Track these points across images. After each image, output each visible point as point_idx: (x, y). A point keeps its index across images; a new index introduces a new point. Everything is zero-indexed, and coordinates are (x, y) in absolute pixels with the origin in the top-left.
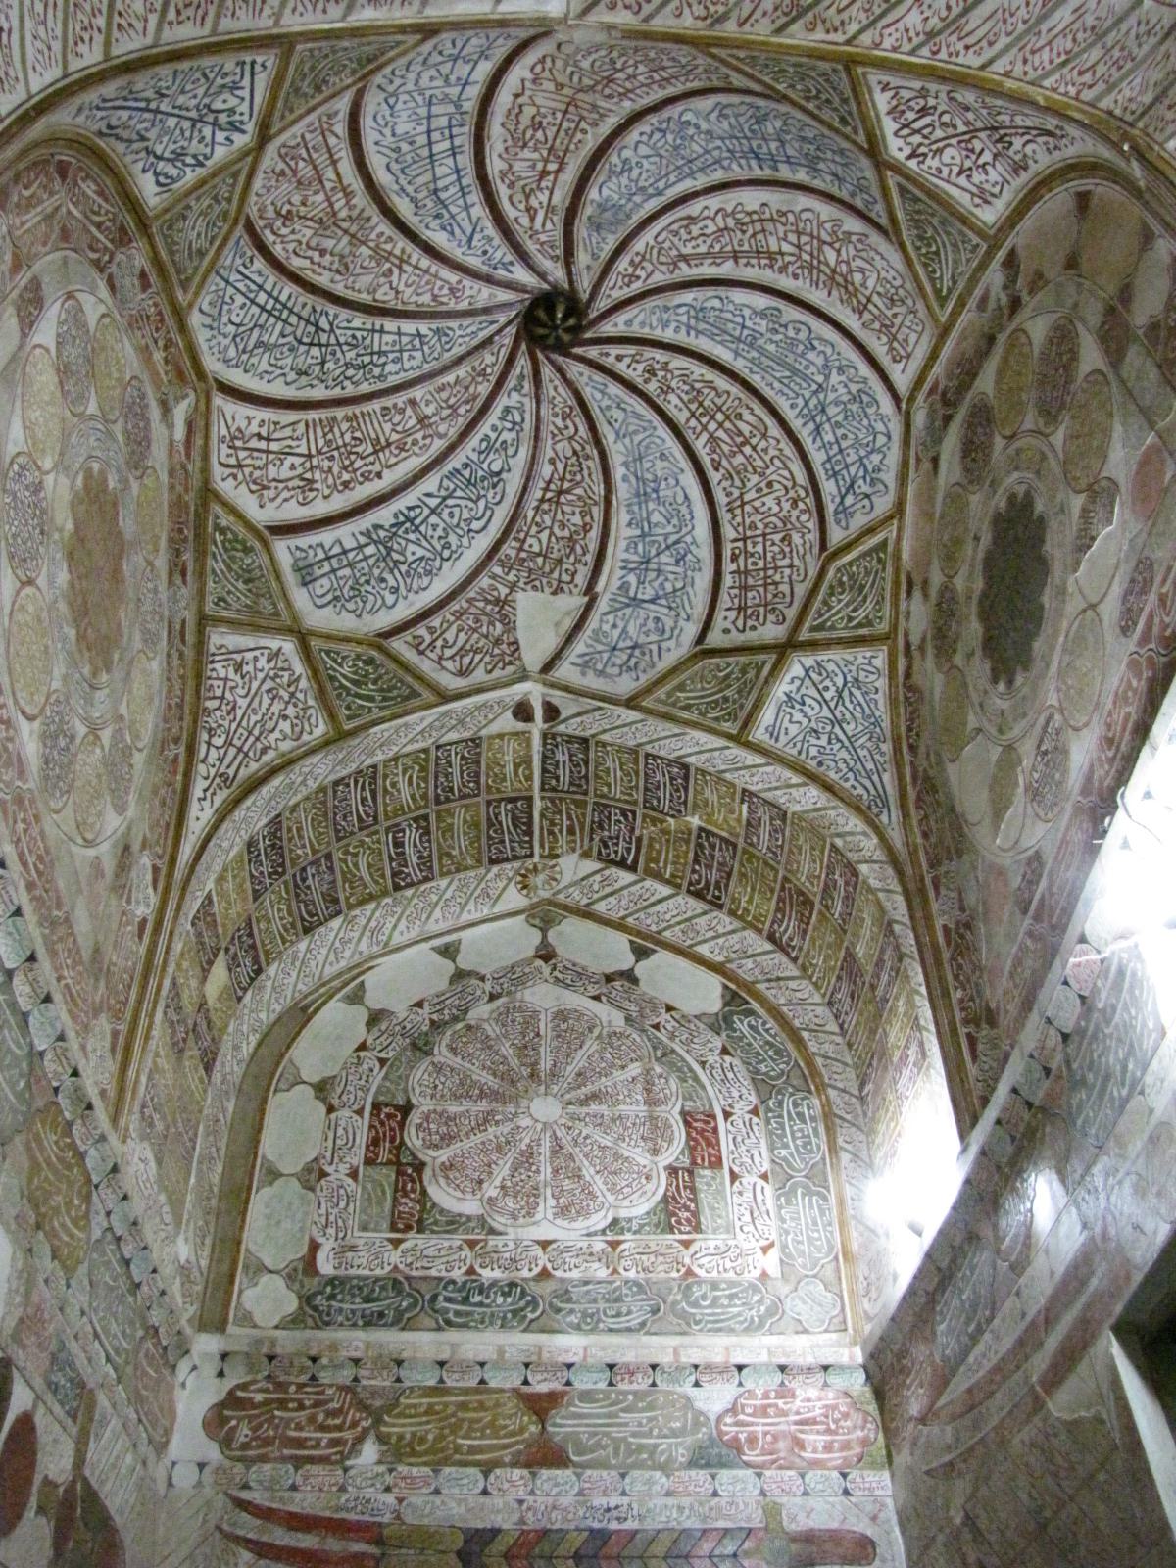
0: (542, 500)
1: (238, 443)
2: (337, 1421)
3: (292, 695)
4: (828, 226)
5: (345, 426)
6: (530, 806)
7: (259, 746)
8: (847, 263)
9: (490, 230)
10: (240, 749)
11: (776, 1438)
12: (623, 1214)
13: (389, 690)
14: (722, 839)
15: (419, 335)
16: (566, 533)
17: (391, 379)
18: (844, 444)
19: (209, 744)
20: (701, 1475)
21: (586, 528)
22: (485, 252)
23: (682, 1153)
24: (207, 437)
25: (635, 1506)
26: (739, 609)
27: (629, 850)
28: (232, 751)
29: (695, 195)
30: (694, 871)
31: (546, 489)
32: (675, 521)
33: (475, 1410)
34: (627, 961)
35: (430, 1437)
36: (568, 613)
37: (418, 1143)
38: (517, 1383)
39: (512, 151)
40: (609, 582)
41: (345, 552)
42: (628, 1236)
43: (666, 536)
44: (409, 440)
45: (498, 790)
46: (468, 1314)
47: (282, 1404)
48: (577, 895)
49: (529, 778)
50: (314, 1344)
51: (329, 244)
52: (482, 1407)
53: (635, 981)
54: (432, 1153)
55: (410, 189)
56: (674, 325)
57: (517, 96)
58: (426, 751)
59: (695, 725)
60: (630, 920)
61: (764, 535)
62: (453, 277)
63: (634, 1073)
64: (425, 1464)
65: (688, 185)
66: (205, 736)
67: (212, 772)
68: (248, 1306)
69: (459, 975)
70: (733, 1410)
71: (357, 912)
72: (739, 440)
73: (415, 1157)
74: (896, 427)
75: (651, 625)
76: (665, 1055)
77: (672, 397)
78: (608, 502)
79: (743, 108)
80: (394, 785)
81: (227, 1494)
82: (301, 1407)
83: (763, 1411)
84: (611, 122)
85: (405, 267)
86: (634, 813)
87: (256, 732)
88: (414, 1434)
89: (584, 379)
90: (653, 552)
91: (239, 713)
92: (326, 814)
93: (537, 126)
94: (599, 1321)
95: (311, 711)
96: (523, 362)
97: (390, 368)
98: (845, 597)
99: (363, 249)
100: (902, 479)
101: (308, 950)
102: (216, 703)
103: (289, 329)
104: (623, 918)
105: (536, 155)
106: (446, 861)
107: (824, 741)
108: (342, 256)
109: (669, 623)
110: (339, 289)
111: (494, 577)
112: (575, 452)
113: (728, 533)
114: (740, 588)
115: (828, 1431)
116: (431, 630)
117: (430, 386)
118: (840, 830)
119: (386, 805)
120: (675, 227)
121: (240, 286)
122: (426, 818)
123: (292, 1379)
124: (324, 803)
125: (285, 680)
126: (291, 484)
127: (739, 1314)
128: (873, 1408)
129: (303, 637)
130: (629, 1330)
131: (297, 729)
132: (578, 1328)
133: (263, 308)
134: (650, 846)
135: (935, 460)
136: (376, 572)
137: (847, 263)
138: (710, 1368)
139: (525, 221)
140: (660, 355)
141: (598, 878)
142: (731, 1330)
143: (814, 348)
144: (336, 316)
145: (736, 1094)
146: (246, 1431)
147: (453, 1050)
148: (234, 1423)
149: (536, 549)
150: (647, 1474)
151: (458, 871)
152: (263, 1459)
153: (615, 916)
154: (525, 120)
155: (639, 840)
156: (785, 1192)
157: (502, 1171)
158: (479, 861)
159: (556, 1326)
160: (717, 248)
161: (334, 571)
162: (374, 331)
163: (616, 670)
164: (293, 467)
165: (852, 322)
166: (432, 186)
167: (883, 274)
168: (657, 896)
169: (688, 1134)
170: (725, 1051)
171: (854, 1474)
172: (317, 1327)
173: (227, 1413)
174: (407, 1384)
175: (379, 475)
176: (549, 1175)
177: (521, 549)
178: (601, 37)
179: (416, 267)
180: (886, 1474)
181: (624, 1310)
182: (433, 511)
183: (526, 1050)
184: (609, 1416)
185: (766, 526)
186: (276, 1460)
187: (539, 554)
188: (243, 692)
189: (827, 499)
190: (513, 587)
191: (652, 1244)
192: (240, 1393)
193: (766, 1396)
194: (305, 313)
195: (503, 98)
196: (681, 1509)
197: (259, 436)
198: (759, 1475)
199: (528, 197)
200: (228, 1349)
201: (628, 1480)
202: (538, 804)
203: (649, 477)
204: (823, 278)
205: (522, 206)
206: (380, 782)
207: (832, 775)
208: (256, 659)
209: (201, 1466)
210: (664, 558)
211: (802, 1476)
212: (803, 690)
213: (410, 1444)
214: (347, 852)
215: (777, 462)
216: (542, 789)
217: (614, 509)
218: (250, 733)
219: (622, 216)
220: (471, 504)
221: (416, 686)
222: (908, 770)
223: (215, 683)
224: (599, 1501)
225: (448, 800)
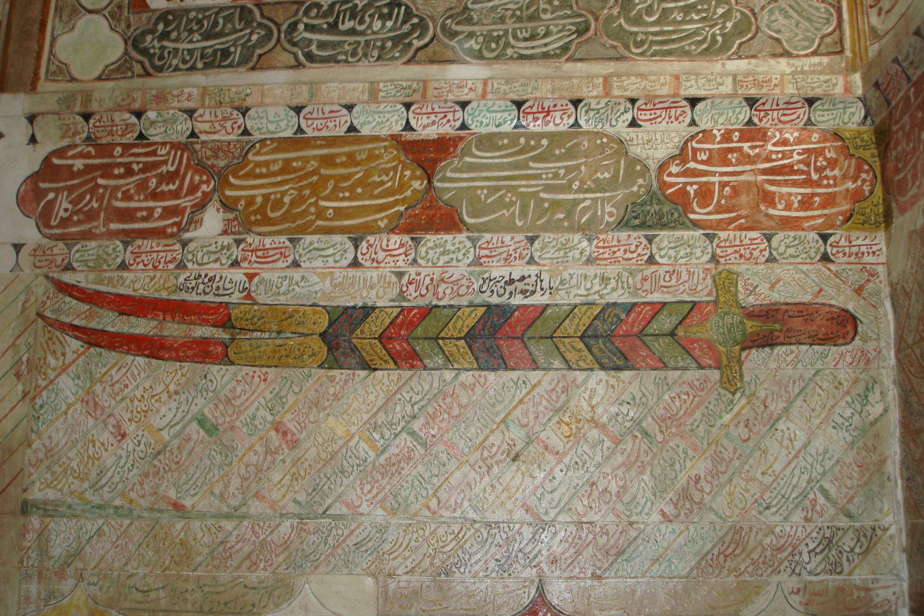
2: (172, 187)
11: (736, 192)
20: (636, 237)
25: (545, 276)
33: (343, 165)
35: (287, 200)
38: (397, 128)
46: (339, 44)
47: (106, 171)
50: (137, 95)
52: (351, 160)
64: (279, 233)
68: (62, 52)
70: (682, 155)
81: (47, 277)
82: (129, 172)
83: (722, 157)
88: (266, 197)
94: (507, 44)
115: (808, 182)
123: (118, 140)
127: (696, 32)
128: (870, 154)
130: (546, 56)
132: (479, 56)
138: (650, 99)
142: (685, 54)
146: (65, 205)
148: (51, 196)
150: (563, 238)
152: (87, 236)
159: (449, 54)
171: (838, 236)
172: (148, 74)
173: (43, 185)
174: (257, 136)
180: (881, 236)
181: (541, 31)
184: (516, 166)
186: (101, 236)
192: (56, 161)
193: (727, 136)
196: (605, 280)
198: (710, 237)
200: (36, 110)
201: (536, 245)
209: (18, 247)
211: (769, 238)
213: (262, 210)
224: (499, 271)
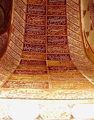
45: (46, 2)
58: (27, 15)
71: (68, 33)
80: (35, 22)
92: (35, 36)
119: (41, 24)
124: (30, 36)
151: (66, 11)
158: (64, 7)
206: (32, 25)
214: (49, 33)
225: (45, 12)
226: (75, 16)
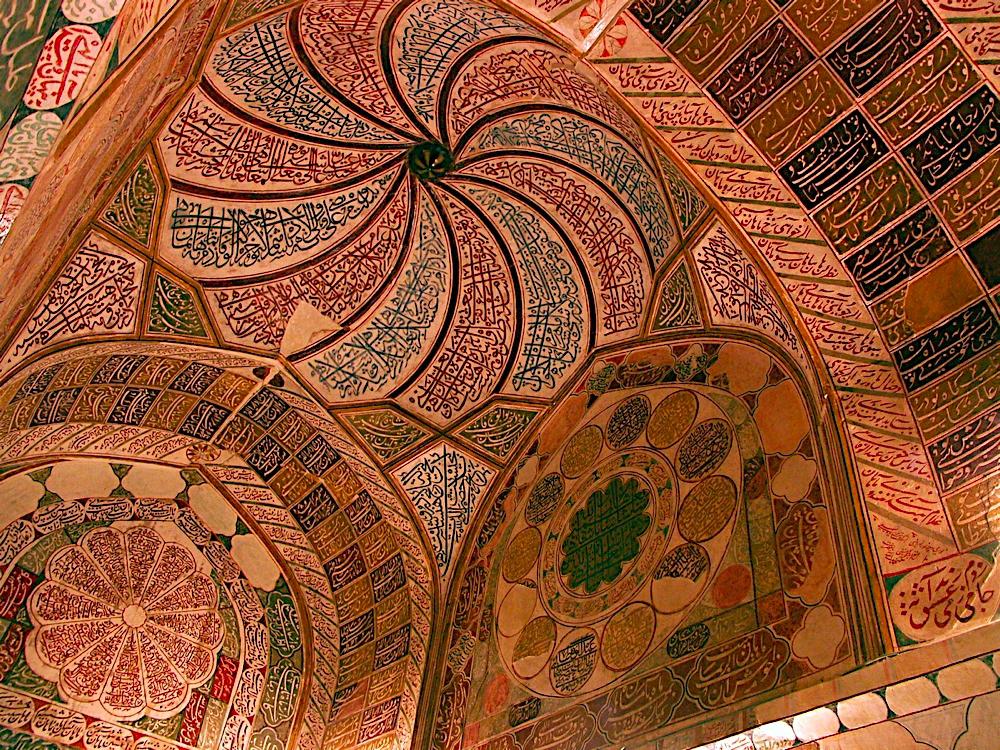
0: (351, 254)
1: (190, 121)
3: (123, 297)
4: (624, 238)
5: (263, 142)
6: (226, 416)
7: (81, 321)
8: (619, 261)
9: (434, 95)
10: (66, 319)
12: (153, 714)
13: (188, 322)
14: (332, 499)
15: (347, 119)
16: (353, 282)
17: (311, 131)
18: (545, 343)
19: (46, 307)
21: (367, 287)
22: (422, 103)
23: (207, 683)
24: (173, 110)
26: (427, 391)
27: (269, 468)
28: (61, 318)
29: (566, 164)
30: (302, 503)
31: (358, 249)
32: (421, 316)
34: (231, 530)
36: (325, 331)
37: (36, 609)
39: (484, 70)
40: (360, 327)
41: (212, 217)
42: (149, 732)
43: (411, 321)
44: (296, 171)
48: (221, 473)
49: (237, 403)
51: (335, 42)
53: (229, 547)
54: (41, 619)
55: (408, 46)
56: (496, 211)
57: (513, 52)
58: (185, 362)
59: (362, 446)
60: (246, 505)
61: (467, 358)
62: (391, 102)
63: (201, 613)
65: (565, 156)
66: (47, 302)
67: (38, 328)
69: (120, 491)
72: (488, 296)
73: (28, 620)
74: (581, 359)
75: (369, 367)
76: (226, 607)
77: (467, 247)
78: (389, 280)
79: (630, 157)
84: (555, 102)
85: (369, 80)
86: (288, 455)
87: (84, 312)
89: (424, 203)
90: (397, 325)
91: (80, 293)
93: (510, 70)
95: (130, 314)
96: (395, 170)
97: (316, 125)
98: (492, 427)
99: (353, 57)
100: (567, 387)
101: (26, 436)
102: (69, 280)
103: (272, 71)
104: (242, 502)
105: (496, 82)
106: (153, 419)
107: (431, 501)
108: (337, 53)
109: (381, 373)
110: (320, 68)
111: (293, 282)
112: (389, 239)
113: (448, 343)
114: (435, 379)
116: (235, 294)
117: (331, 149)
118: (410, 552)
120: (539, 167)
121: (262, 36)
122: (157, 392)
125: (124, 285)
126: (204, 159)
129: (152, 261)
131: (113, 322)
133: (265, 52)
134: (284, 474)
135: (593, 399)
136: (223, 239)
137: (619, 261)
139: (458, 104)
140: (477, 221)
141: (240, 471)
143: (565, 282)
144: (306, 80)
145: (257, 653)
147: (91, 546)
149: (329, 280)
151: (156, 427)
153: (237, 497)
154: (507, 64)
155: (279, 468)
156: (258, 735)
157: (85, 653)
160: (553, 194)
161: (197, 227)
162: (322, 100)
163: (334, 384)
164: (213, 150)
165: (597, 290)
166: (422, 54)
167: (634, 283)
168: (270, 502)
169: (217, 670)
170: (262, 621)
175: (263, 182)
176: (116, 667)
177: (320, 275)
178: (595, 80)
179: (376, 84)
182: (282, 221)
183: (140, 565)
185: (472, 354)
187: (328, 285)
188: (91, 281)
189: (516, 365)
190: (302, 295)
191: (161, 744)
194: (288, 69)
195: (506, 48)
197: (205, 122)
199: (471, 95)
202: (232, 417)
203: (423, 281)
204: (599, 255)
205: (463, 97)
207: (426, 523)
208: (113, 263)
210: (401, 332)
212: (436, 464)
215: (501, 323)
216: (241, 412)
217: (390, 286)
218: (79, 310)
219: (515, 140)
220: (307, 230)
221: (207, 329)
222: (471, 552)
223: (75, 267)
225: (178, 389)
226: (127, 446)
